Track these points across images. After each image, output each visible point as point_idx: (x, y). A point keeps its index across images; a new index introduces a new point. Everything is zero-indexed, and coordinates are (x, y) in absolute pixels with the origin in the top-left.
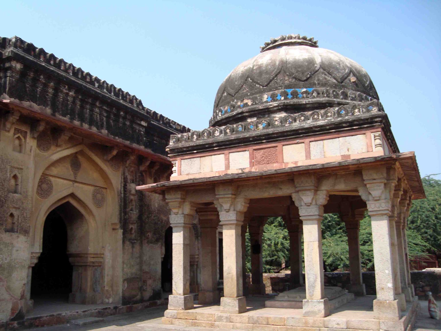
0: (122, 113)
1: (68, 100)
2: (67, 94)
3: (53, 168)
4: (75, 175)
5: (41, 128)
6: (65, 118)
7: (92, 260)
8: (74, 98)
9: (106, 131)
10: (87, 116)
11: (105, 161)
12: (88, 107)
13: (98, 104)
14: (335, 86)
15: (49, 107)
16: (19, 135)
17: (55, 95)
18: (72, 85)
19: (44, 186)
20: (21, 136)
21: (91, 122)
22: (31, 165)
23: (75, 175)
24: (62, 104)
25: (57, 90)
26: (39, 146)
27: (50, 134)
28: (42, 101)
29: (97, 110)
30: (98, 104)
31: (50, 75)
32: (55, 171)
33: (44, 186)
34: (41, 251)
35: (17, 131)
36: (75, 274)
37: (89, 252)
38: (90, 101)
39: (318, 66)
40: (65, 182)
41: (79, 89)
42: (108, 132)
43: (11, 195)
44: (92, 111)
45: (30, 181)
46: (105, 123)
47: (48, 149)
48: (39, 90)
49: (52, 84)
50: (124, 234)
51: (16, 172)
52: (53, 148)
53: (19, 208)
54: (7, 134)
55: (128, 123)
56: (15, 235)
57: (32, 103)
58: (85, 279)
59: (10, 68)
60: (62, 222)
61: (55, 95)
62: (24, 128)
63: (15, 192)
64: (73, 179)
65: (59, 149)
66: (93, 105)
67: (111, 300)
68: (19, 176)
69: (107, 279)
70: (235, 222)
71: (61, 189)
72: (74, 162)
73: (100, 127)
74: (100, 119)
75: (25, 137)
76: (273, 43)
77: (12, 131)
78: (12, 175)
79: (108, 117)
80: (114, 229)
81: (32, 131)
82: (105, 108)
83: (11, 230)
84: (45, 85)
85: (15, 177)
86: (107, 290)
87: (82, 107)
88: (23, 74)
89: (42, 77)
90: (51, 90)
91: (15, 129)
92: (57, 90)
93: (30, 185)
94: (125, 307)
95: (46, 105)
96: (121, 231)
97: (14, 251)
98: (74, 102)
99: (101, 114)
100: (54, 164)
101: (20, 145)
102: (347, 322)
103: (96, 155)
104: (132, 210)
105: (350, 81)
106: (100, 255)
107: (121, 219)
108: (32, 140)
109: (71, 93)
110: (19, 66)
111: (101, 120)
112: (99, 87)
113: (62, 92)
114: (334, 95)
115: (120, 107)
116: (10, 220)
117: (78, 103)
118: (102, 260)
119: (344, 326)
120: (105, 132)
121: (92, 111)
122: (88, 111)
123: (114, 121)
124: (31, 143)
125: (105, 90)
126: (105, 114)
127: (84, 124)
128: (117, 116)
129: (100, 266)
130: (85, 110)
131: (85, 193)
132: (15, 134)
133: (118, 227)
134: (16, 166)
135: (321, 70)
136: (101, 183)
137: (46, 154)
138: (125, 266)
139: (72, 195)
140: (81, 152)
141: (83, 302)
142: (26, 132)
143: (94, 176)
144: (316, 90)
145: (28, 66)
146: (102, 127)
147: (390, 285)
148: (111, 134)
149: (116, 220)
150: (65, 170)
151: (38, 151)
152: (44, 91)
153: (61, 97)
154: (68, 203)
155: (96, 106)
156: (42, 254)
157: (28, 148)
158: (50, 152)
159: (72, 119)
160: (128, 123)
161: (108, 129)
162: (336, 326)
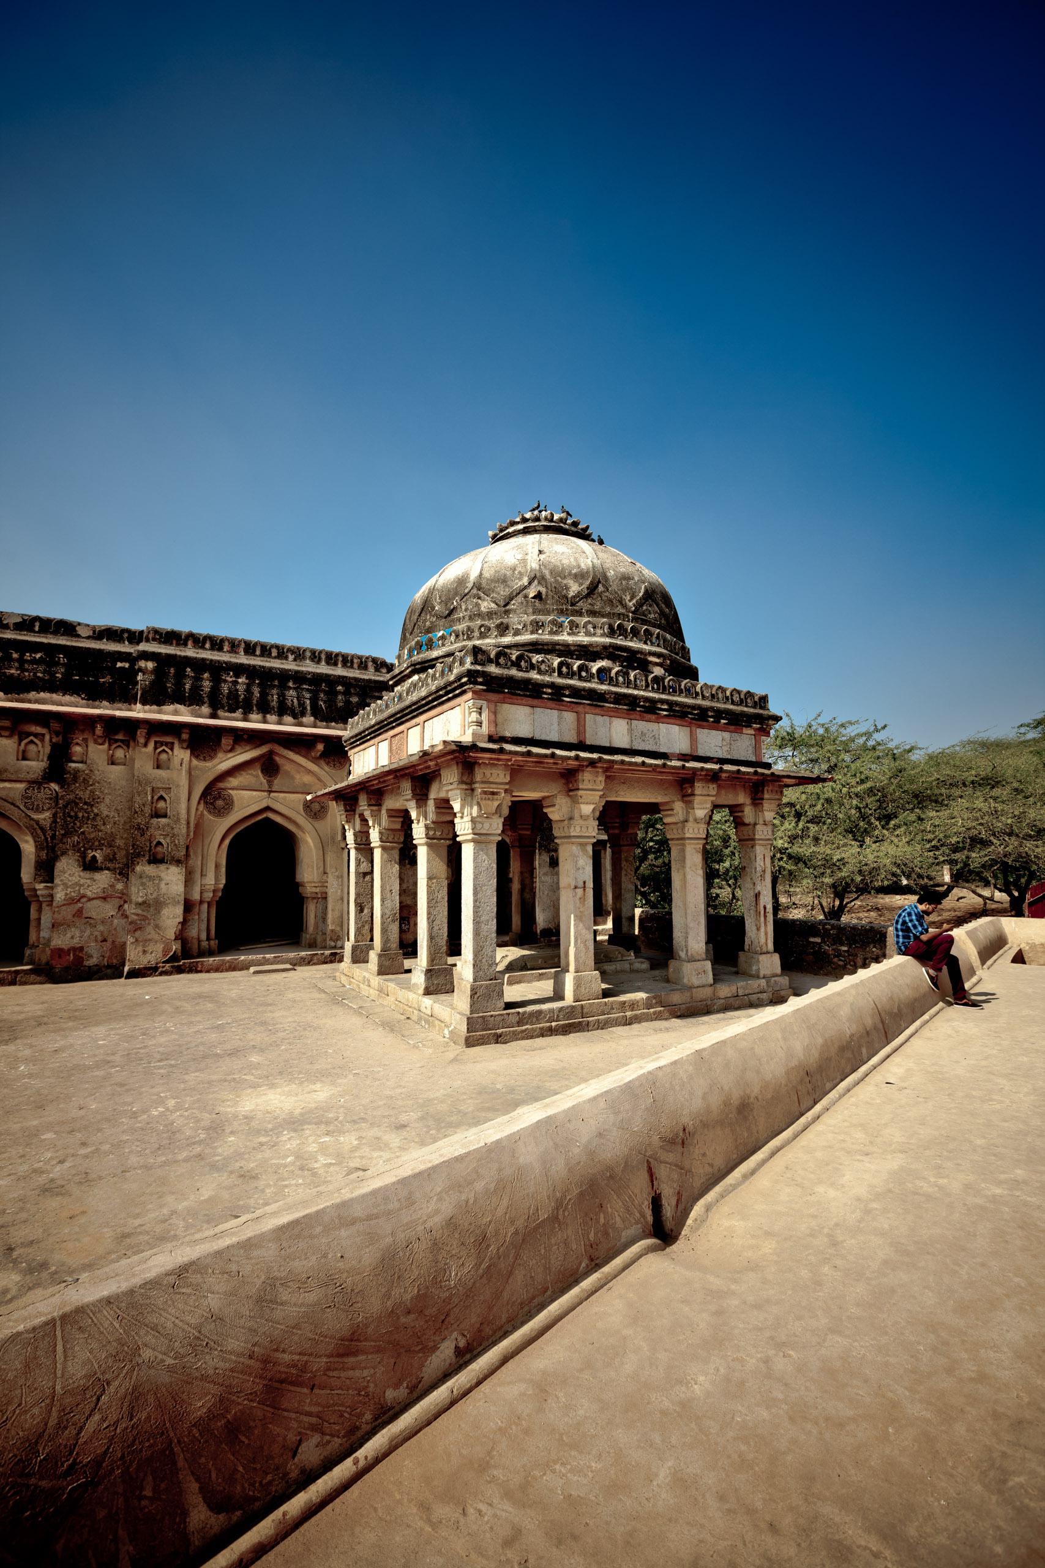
1: (237, 690)
2: (235, 683)
3: (231, 779)
4: (270, 783)
8: (249, 687)
9: (312, 719)
10: (274, 704)
11: (315, 760)
12: (275, 691)
14: (490, 615)
16: (164, 747)
21: (283, 710)
22: (184, 782)
23: (270, 783)
24: (228, 698)
25: (217, 680)
27: (203, 741)
28: (193, 699)
29: (292, 693)
30: (291, 684)
31: (201, 666)
32: (233, 782)
33: (220, 803)
34: (224, 881)
39: (470, 585)
40: (255, 793)
42: (316, 718)
43: (155, 821)
45: (183, 803)
48: (187, 686)
49: (206, 675)
51: (162, 793)
56: (163, 867)
59: (140, 670)
62: (169, 739)
63: (165, 816)
66: (284, 687)
70: (470, 837)
72: (269, 767)
73: (297, 715)
74: (299, 703)
75: (172, 749)
77: (151, 745)
78: (156, 797)
79: (314, 701)
81: (181, 741)
83: (161, 861)
84: (198, 679)
86: (332, 931)
91: (156, 742)
93: (183, 806)
95: (199, 702)
97: (163, 885)
98: (248, 690)
103: (297, 753)
105: (526, 597)
106: (323, 884)
108: (182, 751)
109: (240, 680)
110: (150, 665)
111: (302, 705)
112: (295, 660)
113: (225, 681)
114: (481, 633)
115: (331, 681)
118: (324, 889)
120: (309, 719)
122: (275, 697)
123: (325, 702)
126: (308, 696)
127: (268, 716)
128: (332, 694)
130: (270, 698)
131: (288, 806)
132: (156, 748)
134: (160, 785)
135: (475, 591)
137: (209, 764)
139: (268, 809)
140: (271, 753)
142: (173, 743)
144: (454, 631)
146: (303, 714)
148: (321, 721)
150: (255, 776)
151: (195, 762)
152: (196, 688)
153: (225, 689)
154: (267, 819)
155: (290, 688)
156: (225, 885)
157: (176, 761)
161: (313, 715)
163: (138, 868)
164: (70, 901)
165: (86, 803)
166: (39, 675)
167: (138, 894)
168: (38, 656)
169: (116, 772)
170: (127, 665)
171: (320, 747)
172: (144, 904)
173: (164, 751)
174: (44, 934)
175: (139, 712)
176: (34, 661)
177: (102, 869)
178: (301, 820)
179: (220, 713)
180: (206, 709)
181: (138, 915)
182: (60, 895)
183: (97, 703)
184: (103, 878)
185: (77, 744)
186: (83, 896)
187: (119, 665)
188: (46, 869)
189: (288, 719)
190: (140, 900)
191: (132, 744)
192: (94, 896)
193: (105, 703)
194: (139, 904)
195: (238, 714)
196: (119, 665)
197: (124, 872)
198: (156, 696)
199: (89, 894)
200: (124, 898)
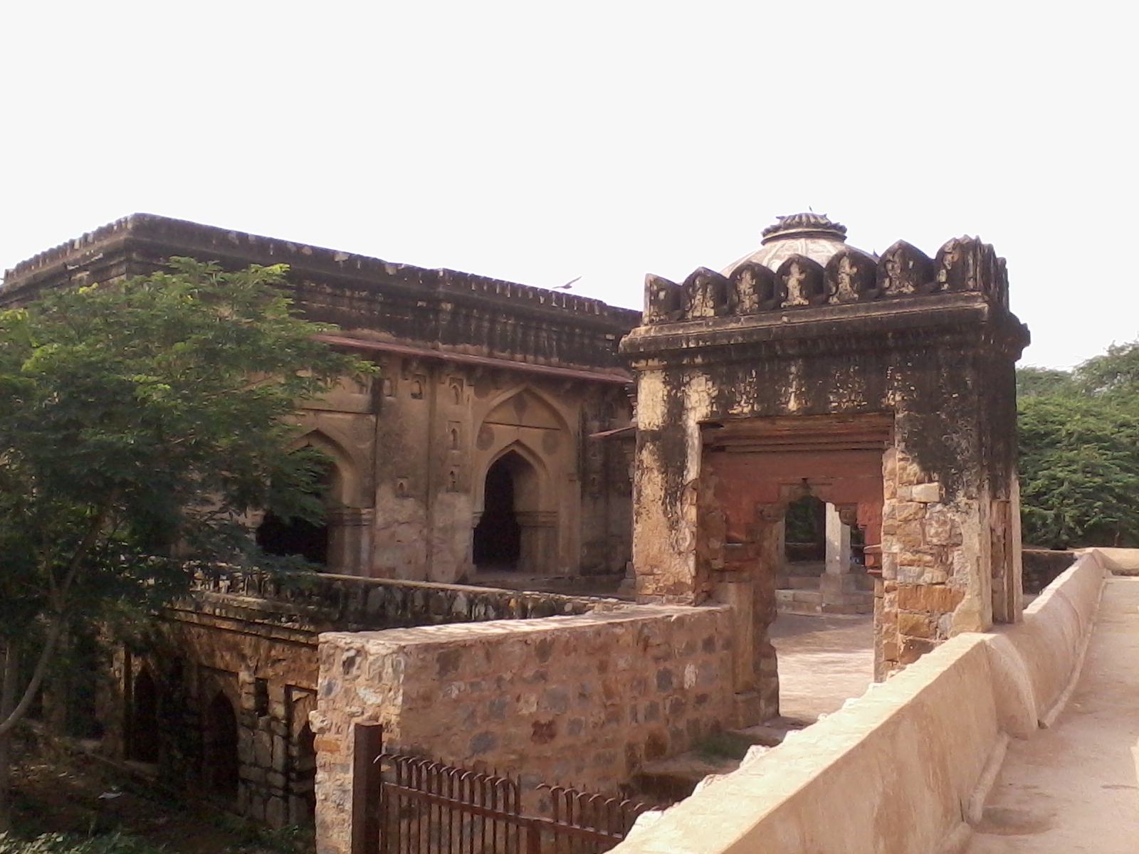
0: (577, 330)
5: (479, 373)
6: (503, 354)
7: (544, 520)
8: (515, 326)
13: (544, 326)
15: (486, 344)
17: (492, 329)
18: (510, 313)
19: (485, 437)
20: (458, 387)
21: (537, 351)
22: (469, 415)
25: (493, 321)
26: (476, 393)
29: (544, 334)
33: (485, 436)
34: (483, 510)
35: (453, 380)
36: (523, 538)
37: (541, 510)
38: (534, 324)
40: (508, 427)
41: (519, 315)
44: (537, 337)
46: (555, 349)
47: (487, 395)
50: (583, 487)
51: (454, 426)
52: (493, 391)
53: (458, 466)
54: (443, 386)
55: (586, 341)
57: (468, 346)
58: (535, 543)
60: (506, 475)
61: (492, 329)
62: (459, 376)
63: (455, 447)
64: (518, 424)
65: (499, 392)
66: (539, 329)
67: (567, 570)
68: (457, 430)
69: (561, 542)
71: (504, 437)
76: (775, 232)
79: (559, 340)
80: (571, 481)
81: (468, 379)
82: (554, 329)
84: (480, 319)
85: (454, 431)
87: (524, 334)
88: (454, 313)
89: (475, 311)
90: (486, 324)
92: (493, 321)
94: (583, 578)
96: (578, 485)
98: (514, 331)
99: (549, 338)
100: (495, 409)
101: (457, 395)
102: (794, 595)
104: (594, 455)
106: (554, 513)
107: (579, 466)
108: (468, 388)
110: (449, 306)
111: (550, 345)
116: (450, 479)
117: (520, 331)
119: (791, 599)
120: (555, 360)
121: (537, 337)
124: (468, 392)
125: (554, 304)
126: (555, 337)
129: (553, 527)
131: (533, 439)
132: (450, 385)
133: (575, 478)
136: (553, 423)
137: (484, 400)
138: (585, 527)
139: (518, 442)
141: (534, 570)
143: (543, 416)
145: (458, 303)
146: (551, 355)
147: (838, 558)
149: (573, 470)
150: (509, 414)
153: (498, 328)
157: (465, 397)
158: (490, 397)
159: (513, 353)
160: (586, 341)
162: (783, 598)
163: (440, 496)
164: (387, 526)
165: (397, 434)
166: (363, 312)
167: (440, 520)
168: (364, 294)
169: (417, 408)
170: (424, 304)
171: (568, 386)
172: (444, 530)
173: (455, 387)
174: (364, 556)
175: (444, 351)
176: (361, 299)
177: (408, 496)
178: (541, 454)
179: (497, 353)
180: (485, 349)
181: (438, 538)
182: (380, 520)
183: (403, 340)
184: (410, 503)
185: (388, 379)
186: (397, 521)
187: (420, 304)
188: (371, 497)
189: (541, 359)
190: (441, 525)
191: (428, 380)
192: (404, 521)
193: (409, 340)
194: (440, 529)
195: (506, 354)
196: (420, 304)
197: (426, 500)
198: (452, 339)
199: (400, 519)
200: (428, 522)
